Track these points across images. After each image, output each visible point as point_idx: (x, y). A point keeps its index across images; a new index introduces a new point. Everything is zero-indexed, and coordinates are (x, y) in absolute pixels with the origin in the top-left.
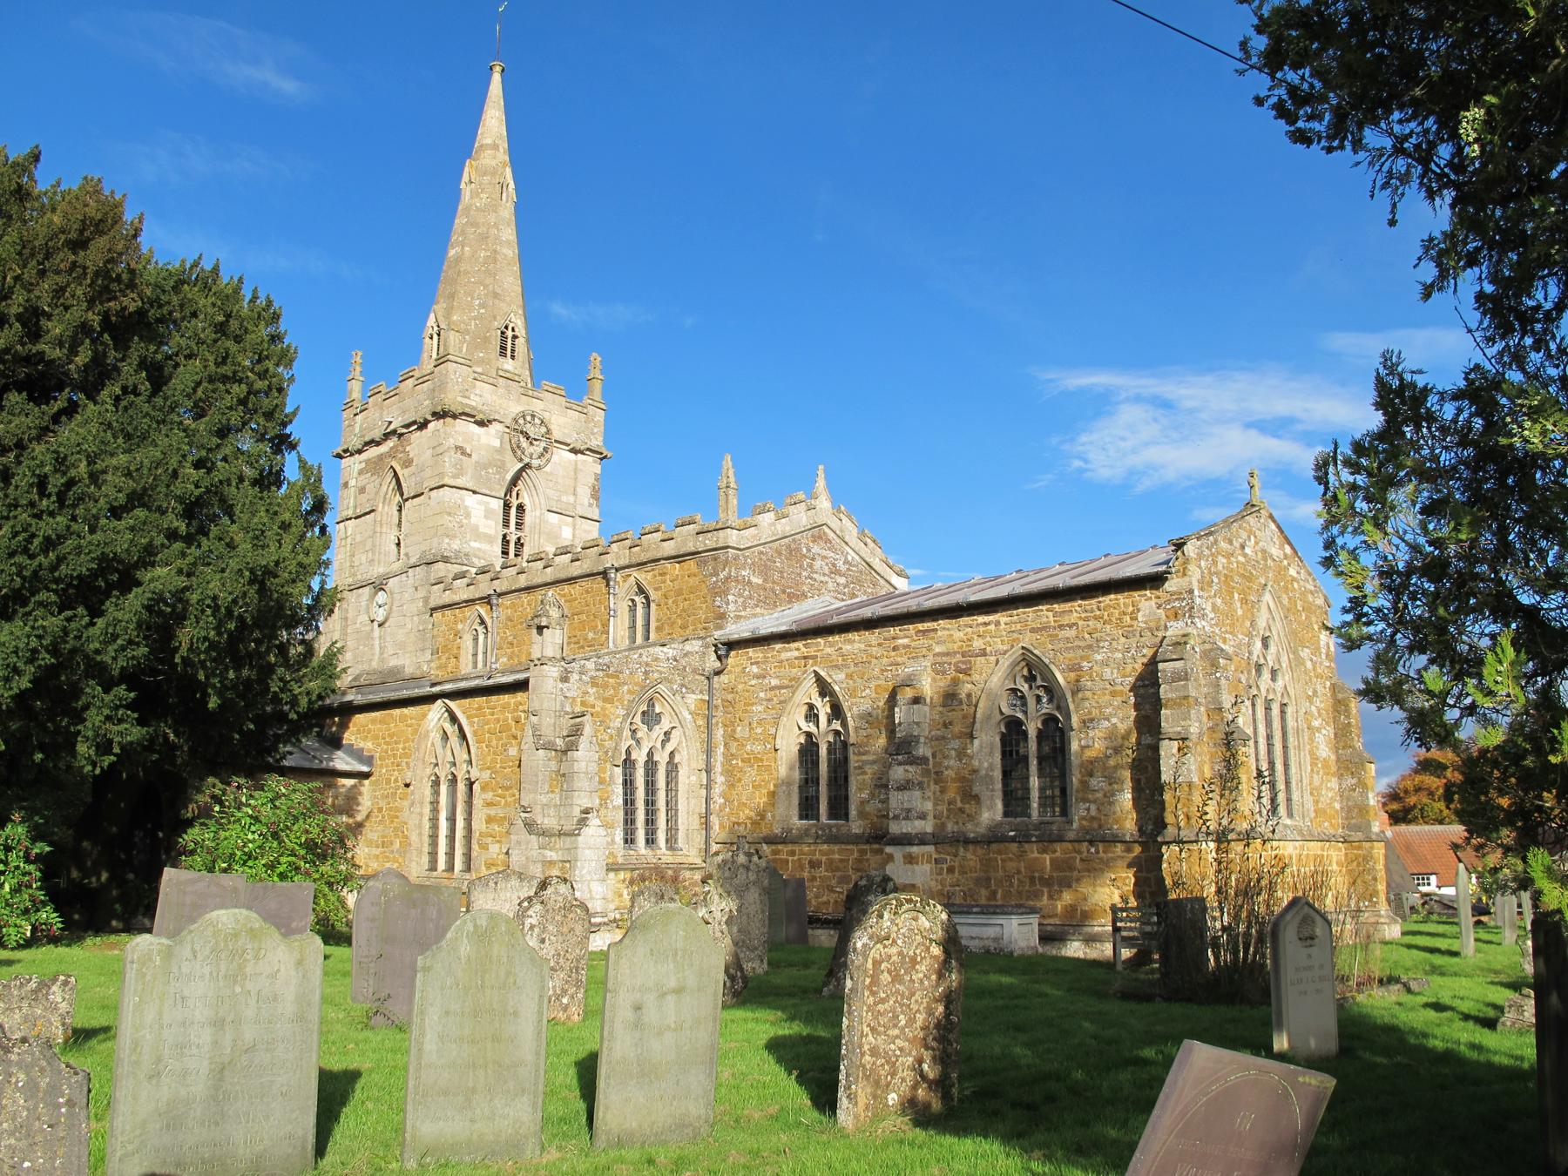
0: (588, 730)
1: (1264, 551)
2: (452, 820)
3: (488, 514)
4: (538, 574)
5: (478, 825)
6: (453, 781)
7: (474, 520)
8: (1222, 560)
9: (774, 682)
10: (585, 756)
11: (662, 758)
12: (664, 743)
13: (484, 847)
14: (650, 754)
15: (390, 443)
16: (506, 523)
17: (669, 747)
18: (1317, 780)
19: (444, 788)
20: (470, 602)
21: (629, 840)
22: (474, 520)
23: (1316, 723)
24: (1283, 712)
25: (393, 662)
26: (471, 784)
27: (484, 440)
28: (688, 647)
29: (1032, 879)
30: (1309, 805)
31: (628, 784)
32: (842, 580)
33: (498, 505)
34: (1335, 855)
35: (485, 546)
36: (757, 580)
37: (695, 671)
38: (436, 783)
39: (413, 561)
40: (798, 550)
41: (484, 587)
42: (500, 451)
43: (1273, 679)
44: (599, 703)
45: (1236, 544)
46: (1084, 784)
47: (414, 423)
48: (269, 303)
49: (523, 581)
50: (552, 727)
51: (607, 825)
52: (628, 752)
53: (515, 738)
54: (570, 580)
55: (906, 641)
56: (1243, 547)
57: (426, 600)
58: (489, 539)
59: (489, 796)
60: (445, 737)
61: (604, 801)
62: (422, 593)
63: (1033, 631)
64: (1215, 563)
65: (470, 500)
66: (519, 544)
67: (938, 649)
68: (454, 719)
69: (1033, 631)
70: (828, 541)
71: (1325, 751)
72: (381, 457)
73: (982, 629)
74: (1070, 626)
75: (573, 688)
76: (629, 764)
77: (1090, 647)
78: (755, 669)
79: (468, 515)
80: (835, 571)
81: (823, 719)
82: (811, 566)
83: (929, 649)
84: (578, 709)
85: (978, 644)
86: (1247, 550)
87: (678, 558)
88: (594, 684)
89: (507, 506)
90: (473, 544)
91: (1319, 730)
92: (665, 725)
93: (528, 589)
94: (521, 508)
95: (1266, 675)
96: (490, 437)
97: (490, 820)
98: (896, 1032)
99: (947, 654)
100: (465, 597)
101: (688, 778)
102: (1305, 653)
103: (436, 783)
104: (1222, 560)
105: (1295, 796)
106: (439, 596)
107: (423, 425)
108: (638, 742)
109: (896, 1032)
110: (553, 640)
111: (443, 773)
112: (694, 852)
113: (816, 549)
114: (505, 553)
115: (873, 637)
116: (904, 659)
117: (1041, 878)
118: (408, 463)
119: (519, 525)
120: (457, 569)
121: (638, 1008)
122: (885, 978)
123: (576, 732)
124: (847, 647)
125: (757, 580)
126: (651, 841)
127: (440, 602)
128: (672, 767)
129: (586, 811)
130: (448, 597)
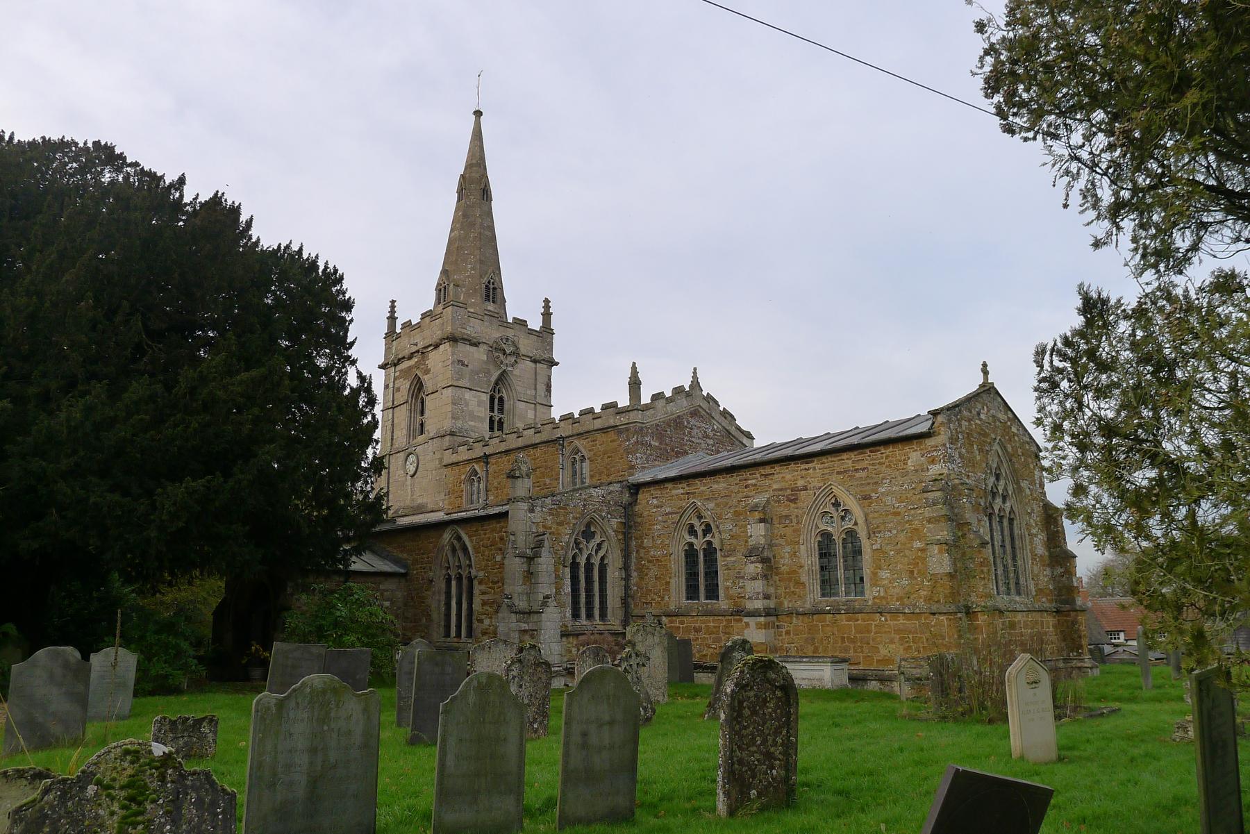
0: (546, 544)
2: (459, 604)
3: (480, 403)
4: (513, 442)
5: (477, 606)
6: (459, 578)
7: (471, 408)
8: (964, 423)
9: (668, 510)
10: (545, 562)
11: (596, 561)
13: (481, 621)
16: (492, 410)
17: (601, 554)
18: (1036, 569)
19: (454, 583)
20: (469, 461)
21: (576, 615)
23: (1034, 531)
25: (420, 501)
26: (470, 580)
27: (476, 355)
28: (611, 488)
29: (843, 638)
31: (575, 579)
32: (711, 442)
33: (486, 398)
34: (1050, 621)
37: (616, 503)
39: (431, 435)
41: (479, 451)
42: (486, 363)
43: (1004, 502)
44: (554, 526)
46: (875, 574)
48: (336, 271)
49: (503, 447)
50: (522, 541)
51: (561, 605)
52: (574, 557)
54: (534, 446)
55: (753, 481)
56: (979, 414)
57: (441, 460)
58: (481, 420)
59: (483, 587)
60: (454, 550)
61: (559, 589)
62: (438, 455)
63: (838, 473)
64: (960, 425)
65: (468, 395)
66: (501, 423)
68: (459, 538)
71: (1041, 550)
72: (410, 368)
73: (804, 472)
74: (863, 470)
75: (537, 516)
76: (575, 566)
77: (876, 483)
78: (655, 501)
79: (467, 405)
81: (700, 533)
83: (769, 486)
84: (541, 530)
85: (801, 483)
86: (982, 416)
87: (603, 430)
88: (551, 514)
89: (492, 399)
91: (1036, 536)
92: (598, 539)
93: (507, 452)
94: (501, 400)
95: (999, 500)
96: (480, 354)
97: (484, 603)
98: (754, 749)
101: (613, 574)
102: (1024, 484)
104: (964, 423)
105: (1022, 581)
106: (449, 457)
107: (437, 346)
108: (580, 550)
109: (754, 749)
110: (523, 487)
111: (453, 574)
112: (618, 622)
113: (693, 422)
114: (491, 429)
115: (734, 478)
118: (427, 372)
119: (501, 411)
120: (460, 440)
121: (585, 734)
122: (747, 712)
123: (539, 545)
124: (715, 486)
126: (590, 616)
129: (547, 597)
130: (455, 458)
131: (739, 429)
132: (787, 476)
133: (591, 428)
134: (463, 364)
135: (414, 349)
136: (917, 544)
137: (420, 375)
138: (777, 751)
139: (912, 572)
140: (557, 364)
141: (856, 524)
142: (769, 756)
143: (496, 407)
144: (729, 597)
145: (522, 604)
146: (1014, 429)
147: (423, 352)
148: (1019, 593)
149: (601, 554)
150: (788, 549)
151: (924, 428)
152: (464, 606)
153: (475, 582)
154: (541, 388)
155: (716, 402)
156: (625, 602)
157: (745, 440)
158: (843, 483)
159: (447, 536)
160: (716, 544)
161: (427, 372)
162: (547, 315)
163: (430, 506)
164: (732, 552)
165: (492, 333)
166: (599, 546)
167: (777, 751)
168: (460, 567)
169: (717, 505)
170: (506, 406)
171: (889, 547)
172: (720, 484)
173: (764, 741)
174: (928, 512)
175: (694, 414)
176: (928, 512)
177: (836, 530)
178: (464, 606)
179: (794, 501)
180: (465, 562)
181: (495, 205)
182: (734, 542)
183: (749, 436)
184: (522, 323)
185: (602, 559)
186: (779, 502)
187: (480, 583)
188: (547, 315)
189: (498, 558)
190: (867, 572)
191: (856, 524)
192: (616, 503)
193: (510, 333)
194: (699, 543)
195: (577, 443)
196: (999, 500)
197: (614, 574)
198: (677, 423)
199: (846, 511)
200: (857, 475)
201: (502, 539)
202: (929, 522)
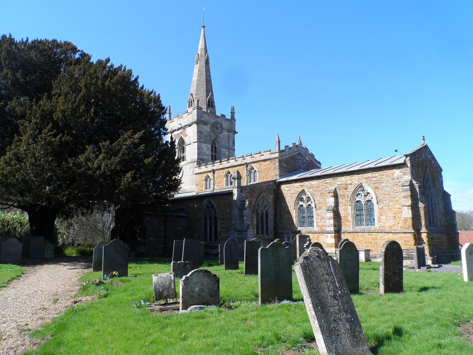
1: (426, 157)
3: (208, 149)
5: (219, 229)
6: (211, 218)
7: (204, 151)
9: (293, 192)
12: (265, 208)
13: (221, 235)
14: (262, 210)
15: (180, 131)
16: (212, 152)
17: (266, 209)
18: (440, 217)
19: (208, 220)
20: (206, 172)
21: (258, 233)
22: (204, 151)
23: (440, 202)
24: (431, 199)
26: (216, 218)
27: (206, 129)
29: (366, 242)
30: (439, 224)
32: (305, 165)
33: (210, 146)
34: (444, 237)
35: (207, 157)
36: (285, 166)
37: (272, 189)
38: (206, 219)
39: (189, 161)
40: (295, 158)
42: (210, 132)
45: (420, 155)
46: (380, 218)
47: (187, 125)
51: (253, 229)
53: (229, 207)
55: (329, 181)
56: (421, 156)
57: (193, 171)
58: (208, 155)
59: (222, 222)
62: (192, 169)
63: (365, 178)
64: (415, 160)
67: (339, 183)
68: (210, 203)
69: (365, 178)
70: (302, 155)
71: (442, 210)
72: (178, 134)
74: (375, 177)
78: (287, 189)
79: (203, 149)
80: (304, 163)
82: (298, 162)
85: (349, 182)
86: (423, 157)
87: (265, 161)
89: (212, 147)
90: (205, 157)
91: (440, 204)
94: (215, 147)
95: (427, 190)
97: (222, 228)
99: (341, 185)
100: (204, 171)
102: (436, 184)
103: (206, 219)
104: (417, 160)
105: (435, 221)
106: (197, 170)
107: (190, 125)
112: (272, 236)
113: (299, 157)
116: (329, 186)
117: (369, 242)
118: (186, 136)
119: (215, 152)
122: (388, 258)
125: (285, 166)
126: (262, 233)
127: (198, 172)
128: (267, 214)
131: (315, 160)
132: (343, 179)
133: (259, 160)
134: (201, 133)
135: (180, 126)
136: (398, 206)
137: (183, 137)
138: (397, 271)
139: (395, 217)
140: (237, 133)
141: (372, 198)
142: (394, 273)
143: (214, 151)
144: (318, 226)
145: (239, 228)
146: (433, 162)
147: (184, 128)
148: (434, 227)
149: (266, 209)
150: (343, 207)
151: (401, 161)
152: (213, 228)
153: (218, 220)
154: (231, 143)
155: (307, 149)
156: (275, 228)
157: (318, 165)
158: (367, 182)
159: (205, 202)
160: (313, 205)
161: (186, 136)
162: (233, 113)
163: (189, 190)
164: (320, 209)
165: (213, 121)
166: (266, 206)
167: (397, 271)
168: (211, 214)
169: (313, 190)
170: (217, 150)
171: (386, 207)
172: (315, 182)
173: (393, 268)
174: (403, 194)
175: (300, 154)
176: (403, 194)
177: (363, 200)
178: (213, 228)
179: (346, 189)
180: (213, 212)
181: (210, 65)
182: (321, 205)
183: (320, 163)
184: (223, 116)
185: (267, 211)
186: (340, 189)
187: (220, 220)
188: (233, 113)
189: (228, 210)
190: (376, 216)
191: (372, 198)
192: (272, 189)
193: (219, 120)
194: (305, 205)
195: (253, 165)
196: (427, 190)
197: (271, 217)
198: (293, 158)
199: (368, 193)
200: (373, 179)
201: (229, 203)
202: (403, 198)
